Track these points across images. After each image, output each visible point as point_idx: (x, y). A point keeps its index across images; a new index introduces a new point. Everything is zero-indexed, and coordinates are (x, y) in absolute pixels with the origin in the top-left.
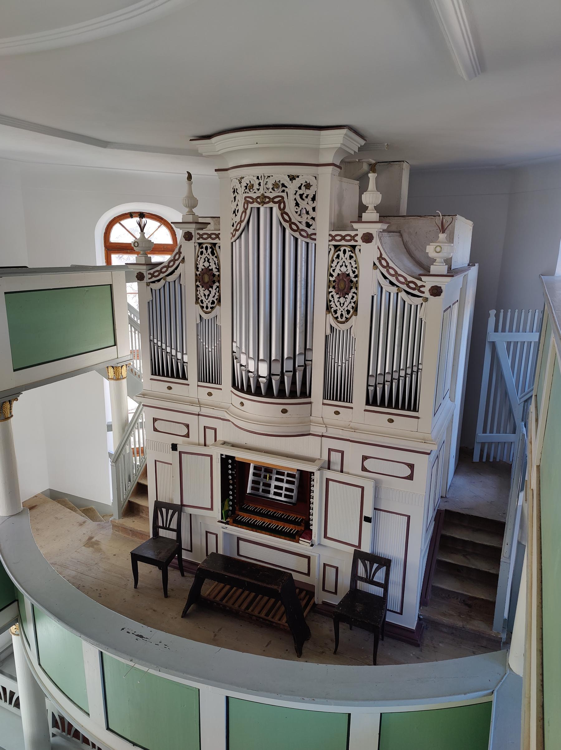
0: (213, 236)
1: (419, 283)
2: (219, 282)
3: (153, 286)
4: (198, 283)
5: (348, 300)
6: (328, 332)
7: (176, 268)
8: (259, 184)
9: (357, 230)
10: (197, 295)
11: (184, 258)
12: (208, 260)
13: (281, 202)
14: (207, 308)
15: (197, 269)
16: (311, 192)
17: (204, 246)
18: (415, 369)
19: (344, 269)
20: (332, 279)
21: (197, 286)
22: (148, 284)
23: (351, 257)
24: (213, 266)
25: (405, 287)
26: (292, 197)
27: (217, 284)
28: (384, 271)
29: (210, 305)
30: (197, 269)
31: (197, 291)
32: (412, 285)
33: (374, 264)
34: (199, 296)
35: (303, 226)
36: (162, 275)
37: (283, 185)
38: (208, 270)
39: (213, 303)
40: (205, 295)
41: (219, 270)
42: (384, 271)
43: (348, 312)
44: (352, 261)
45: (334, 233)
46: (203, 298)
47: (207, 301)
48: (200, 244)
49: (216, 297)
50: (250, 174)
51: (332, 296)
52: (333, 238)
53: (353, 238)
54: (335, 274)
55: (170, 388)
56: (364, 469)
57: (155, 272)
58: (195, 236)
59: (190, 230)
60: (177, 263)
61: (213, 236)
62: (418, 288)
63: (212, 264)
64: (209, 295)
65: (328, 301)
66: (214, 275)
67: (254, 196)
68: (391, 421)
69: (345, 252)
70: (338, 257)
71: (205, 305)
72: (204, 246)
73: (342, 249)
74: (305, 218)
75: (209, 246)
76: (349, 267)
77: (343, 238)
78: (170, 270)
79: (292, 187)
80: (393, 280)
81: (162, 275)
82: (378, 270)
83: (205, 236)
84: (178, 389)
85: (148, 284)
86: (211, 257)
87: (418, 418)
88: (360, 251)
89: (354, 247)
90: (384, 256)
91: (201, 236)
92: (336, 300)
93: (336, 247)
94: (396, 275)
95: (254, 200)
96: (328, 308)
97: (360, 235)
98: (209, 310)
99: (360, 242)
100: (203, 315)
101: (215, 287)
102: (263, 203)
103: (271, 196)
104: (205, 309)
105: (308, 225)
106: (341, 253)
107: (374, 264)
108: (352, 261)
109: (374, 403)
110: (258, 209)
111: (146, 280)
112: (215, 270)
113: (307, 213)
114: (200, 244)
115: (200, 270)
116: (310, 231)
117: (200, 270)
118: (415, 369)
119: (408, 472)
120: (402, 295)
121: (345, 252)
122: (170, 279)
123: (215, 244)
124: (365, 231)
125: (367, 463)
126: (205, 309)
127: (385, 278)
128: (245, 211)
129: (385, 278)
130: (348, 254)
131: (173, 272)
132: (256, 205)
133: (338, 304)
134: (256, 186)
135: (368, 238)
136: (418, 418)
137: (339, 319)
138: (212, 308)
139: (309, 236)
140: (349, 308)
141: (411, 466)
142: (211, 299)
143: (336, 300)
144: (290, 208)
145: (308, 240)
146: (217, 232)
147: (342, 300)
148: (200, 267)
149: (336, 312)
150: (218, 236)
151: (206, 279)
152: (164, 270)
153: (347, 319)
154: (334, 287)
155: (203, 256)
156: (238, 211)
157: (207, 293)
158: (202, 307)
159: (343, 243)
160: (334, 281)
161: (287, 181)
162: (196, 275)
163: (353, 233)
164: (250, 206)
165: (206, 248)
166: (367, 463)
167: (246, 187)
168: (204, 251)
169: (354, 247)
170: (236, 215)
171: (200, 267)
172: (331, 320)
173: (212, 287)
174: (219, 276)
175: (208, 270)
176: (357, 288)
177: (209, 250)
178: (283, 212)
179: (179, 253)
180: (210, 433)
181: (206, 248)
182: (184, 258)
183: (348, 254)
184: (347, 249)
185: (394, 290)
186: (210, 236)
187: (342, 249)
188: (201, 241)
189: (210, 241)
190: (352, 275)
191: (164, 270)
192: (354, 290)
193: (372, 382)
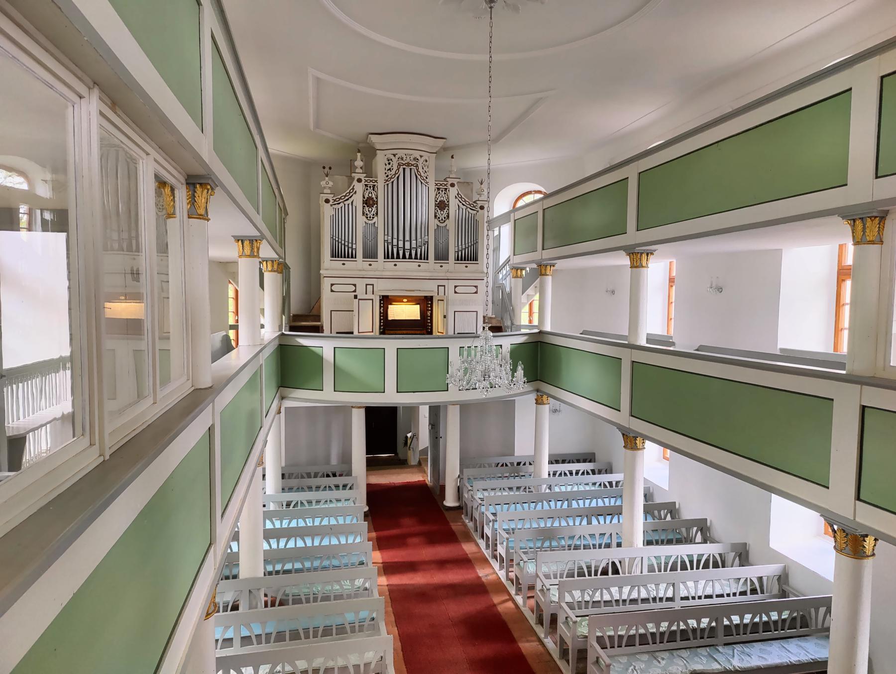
0: (374, 181)
1: (475, 205)
2: (377, 204)
3: (334, 206)
4: (364, 205)
5: (445, 212)
6: (436, 228)
7: (351, 197)
8: (406, 158)
9: (447, 182)
10: (363, 211)
11: (356, 192)
12: (371, 193)
13: (417, 166)
14: (370, 217)
15: (364, 197)
16: (427, 163)
17: (369, 186)
18: (475, 242)
19: (442, 199)
20: (437, 203)
21: (364, 206)
22: (331, 205)
23: (445, 193)
24: (374, 196)
25: (469, 206)
26: (421, 165)
27: (376, 205)
28: (460, 199)
29: (372, 216)
30: (364, 197)
31: (363, 209)
32: (472, 206)
33: (456, 197)
34: (365, 212)
35: (425, 178)
36: (341, 201)
37: (417, 159)
38: (370, 198)
39: (373, 215)
40: (369, 211)
41: (377, 198)
42: (460, 199)
43: (445, 218)
44: (446, 195)
45: (437, 182)
46: (368, 213)
47: (370, 214)
48: (366, 185)
49: (375, 212)
50: (401, 153)
51: (437, 211)
52: (436, 185)
53: (445, 185)
54: (438, 201)
55: (344, 264)
56: (456, 292)
57: (336, 199)
58: (363, 181)
59: (361, 178)
60: (351, 194)
61: (374, 181)
62: (474, 207)
63: (373, 195)
64: (371, 211)
65: (435, 213)
66: (374, 201)
67: (404, 163)
68: (466, 267)
69: (442, 191)
70: (439, 193)
71: (369, 216)
72: (369, 186)
73: (441, 189)
74: (426, 175)
75: (371, 186)
76: (445, 198)
77: (441, 185)
78: (347, 198)
79: (421, 160)
80: (464, 203)
81: (341, 201)
82: (457, 199)
83: (369, 181)
84: (349, 264)
85: (331, 205)
86: (372, 191)
87: (478, 264)
88: (449, 191)
89: (446, 189)
90: (460, 193)
91: (366, 181)
92: (439, 213)
93: (438, 188)
94: (465, 201)
95: (404, 165)
96: (435, 216)
97: (450, 184)
98: (371, 218)
99: (450, 187)
100: (367, 221)
101: (375, 207)
102: (408, 166)
103: (413, 163)
104: (369, 218)
105: (426, 178)
106: (440, 191)
107: (456, 197)
108: (446, 195)
109: (458, 260)
110: (404, 169)
111: (331, 203)
112: (375, 198)
113: (426, 172)
114: (366, 185)
115: (366, 198)
116: (427, 180)
117: (366, 198)
118: (475, 242)
119: (474, 290)
120: (469, 209)
121: (442, 191)
122: (346, 203)
123: (375, 185)
124: (451, 182)
125: (457, 290)
126: (369, 218)
127: (461, 202)
128: (398, 169)
129: (461, 202)
130: (443, 192)
131: (348, 199)
132: (404, 167)
133: (440, 214)
134: (404, 159)
135: (453, 185)
136: (478, 264)
137: (441, 221)
138: (373, 218)
139: (427, 183)
140: (445, 216)
141: (476, 287)
142: (372, 213)
143: (439, 213)
144: (420, 170)
145: (426, 184)
146: (376, 179)
147: (442, 212)
148: (366, 196)
149: (439, 218)
150: (376, 181)
151: (371, 202)
152: (343, 198)
153: (444, 221)
154: (438, 207)
155: (368, 191)
156: (392, 169)
157: (370, 209)
158: (367, 217)
159: (441, 187)
160: (438, 204)
161: (419, 158)
162: (363, 200)
163: (445, 183)
164: (401, 167)
165: (370, 187)
166: (457, 290)
167: (399, 159)
168: (369, 188)
169: (446, 189)
170: (391, 171)
171: (366, 196)
172: (437, 221)
173: (373, 207)
174: (377, 201)
175: (370, 198)
176: (448, 207)
177: (372, 188)
178: (418, 171)
179: (353, 189)
180: (370, 288)
181: (370, 187)
182: (356, 192)
183: (443, 192)
184: (443, 190)
185: (464, 207)
186: (371, 181)
187: (441, 189)
188: (366, 183)
189: (371, 183)
190: (446, 201)
191: (343, 198)
192: (447, 208)
193: (457, 250)
